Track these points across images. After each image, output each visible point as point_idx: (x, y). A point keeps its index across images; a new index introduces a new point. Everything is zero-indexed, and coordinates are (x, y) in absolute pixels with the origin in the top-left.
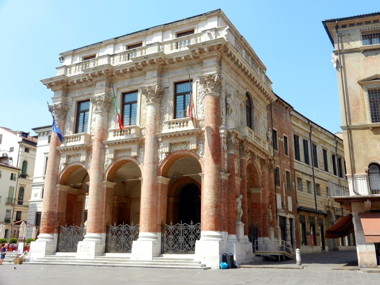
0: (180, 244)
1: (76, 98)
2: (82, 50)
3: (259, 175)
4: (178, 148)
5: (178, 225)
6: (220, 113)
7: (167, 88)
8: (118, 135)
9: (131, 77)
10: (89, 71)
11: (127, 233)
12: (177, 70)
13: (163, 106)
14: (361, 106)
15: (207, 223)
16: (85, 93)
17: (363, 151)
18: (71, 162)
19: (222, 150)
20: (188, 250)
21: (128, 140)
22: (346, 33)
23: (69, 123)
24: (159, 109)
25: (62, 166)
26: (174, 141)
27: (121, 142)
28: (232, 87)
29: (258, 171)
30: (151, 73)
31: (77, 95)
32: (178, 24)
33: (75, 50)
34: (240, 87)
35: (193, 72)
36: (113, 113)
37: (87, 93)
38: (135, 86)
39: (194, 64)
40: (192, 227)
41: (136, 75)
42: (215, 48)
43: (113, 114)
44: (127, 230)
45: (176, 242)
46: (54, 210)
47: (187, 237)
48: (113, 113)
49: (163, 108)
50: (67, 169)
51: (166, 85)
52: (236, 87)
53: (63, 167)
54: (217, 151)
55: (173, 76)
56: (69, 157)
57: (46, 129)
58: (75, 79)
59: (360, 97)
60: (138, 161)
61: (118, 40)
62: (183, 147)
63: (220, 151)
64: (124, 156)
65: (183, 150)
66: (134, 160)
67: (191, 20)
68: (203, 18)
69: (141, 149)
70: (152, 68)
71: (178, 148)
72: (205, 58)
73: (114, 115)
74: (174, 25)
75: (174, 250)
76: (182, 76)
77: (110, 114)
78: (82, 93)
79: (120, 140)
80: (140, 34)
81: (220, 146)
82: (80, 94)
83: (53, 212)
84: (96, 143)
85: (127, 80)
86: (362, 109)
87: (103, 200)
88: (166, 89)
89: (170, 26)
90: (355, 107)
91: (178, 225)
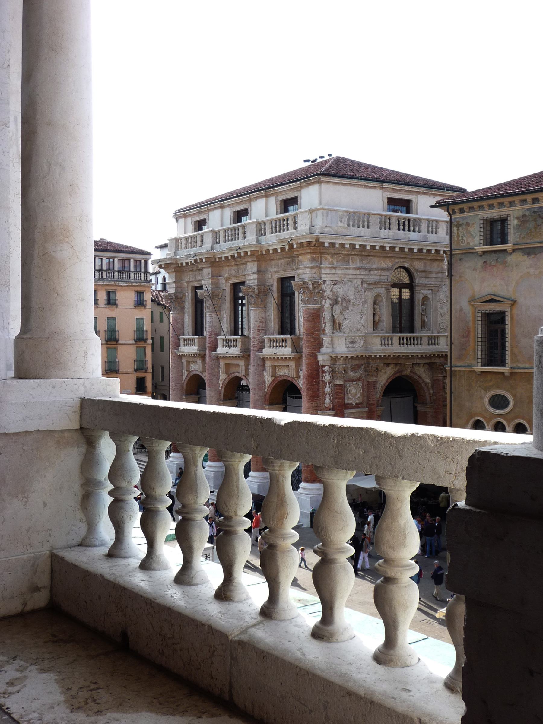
3: (425, 388)
6: (319, 331)
13: (268, 311)
19: (321, 382)
24: (263, 315)
28: (351, 281)
29: (421, 381)
31: (191, 280)
34: (372, 272)
50: (189, 377)
52: (362, 277)
54: (314, 385)
55: (275, 269)
63: (318, 383)
76: (284, 270)
78: (196, 278)
81: (318, 378)
90: (464, 340)
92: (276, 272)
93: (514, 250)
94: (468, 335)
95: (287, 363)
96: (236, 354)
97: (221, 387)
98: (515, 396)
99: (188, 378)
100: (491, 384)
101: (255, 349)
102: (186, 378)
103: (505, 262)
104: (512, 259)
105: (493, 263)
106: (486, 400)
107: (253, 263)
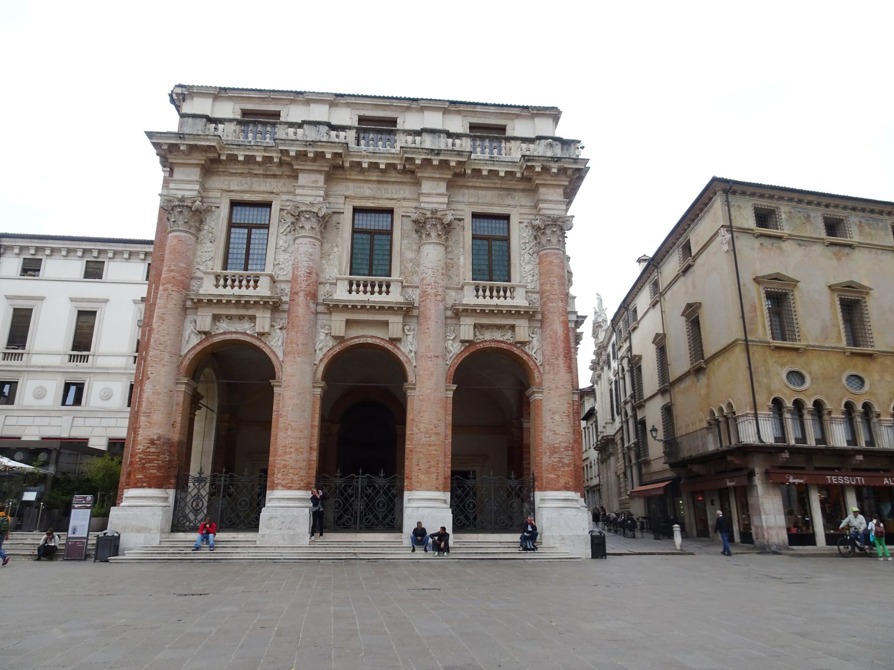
0: (356, 513)
4: (488, 336)
5: (352, 478)
7: (460, 220)
8: (358, 292)
9: (379, 182)
10: (291, 145)
11: (370, 491)
12: (481, 193)
14: (759, 313)
15: (558, 476)
16: (258, 189)
17: (765, 380)
18: (222, 331)
20: (373, 524)
21: (386, 306)
22: (736, 204)
23: (209, 244)
25: (192, 336)
26: (485, 321)
27: (368, 305)
30: (434, 184)
32: (479, 109)
33: (225, 89)
35: (512, 203)
36: (334, 244)
37: (263, 188)
38: (387, 201)
39: (515, 190)
40: (380, 481)
41: (393, 180)
42: (570, 172)
44: (370, 487)
45: (347, 509)
46: (171, 435)
47: (461, 502)
48: (334, 244)
49: (450, 256)
50: (206, 344)
51: (459, 214)
53: (195, 340)
55: (472, 200)
56: (216, 318)
57: (127, 245)
58: (242, 153)
59: (757, 301)
60: (399, 349)
61: (342, 101)
62: (498, 335)
64: (364, 336)
65: (499, 341)
66: (390, 347)
68: (525, 113)
69: (407, 327)
70: (437, 176)
71: (488, 336)
72: (545, 185)
73: (336, 249)
75: (249, 524)
76: (491, 205)
77: (326, 246)
79: (368, 301)
82: (245, 187)
83: (169, 439)
84: (302, 298)
85: (369, 185)
86: (759, 319)
87: (313, 420)
88: (456, 222)
91: (352, 478)
92: (470, 204)
93: (788, 239)
94: (755, 311)
95: (510, 322)
96: (397, 303)
97: (321, 361)
98: (810, 373)
99: (200, 348)
100: (785, 360)
101: (439, 298)
102: (194, 347)
103: (780, 248)
104: (787, 246)
105: (770, 246)
106: (784, 376)
107: (435, 183)
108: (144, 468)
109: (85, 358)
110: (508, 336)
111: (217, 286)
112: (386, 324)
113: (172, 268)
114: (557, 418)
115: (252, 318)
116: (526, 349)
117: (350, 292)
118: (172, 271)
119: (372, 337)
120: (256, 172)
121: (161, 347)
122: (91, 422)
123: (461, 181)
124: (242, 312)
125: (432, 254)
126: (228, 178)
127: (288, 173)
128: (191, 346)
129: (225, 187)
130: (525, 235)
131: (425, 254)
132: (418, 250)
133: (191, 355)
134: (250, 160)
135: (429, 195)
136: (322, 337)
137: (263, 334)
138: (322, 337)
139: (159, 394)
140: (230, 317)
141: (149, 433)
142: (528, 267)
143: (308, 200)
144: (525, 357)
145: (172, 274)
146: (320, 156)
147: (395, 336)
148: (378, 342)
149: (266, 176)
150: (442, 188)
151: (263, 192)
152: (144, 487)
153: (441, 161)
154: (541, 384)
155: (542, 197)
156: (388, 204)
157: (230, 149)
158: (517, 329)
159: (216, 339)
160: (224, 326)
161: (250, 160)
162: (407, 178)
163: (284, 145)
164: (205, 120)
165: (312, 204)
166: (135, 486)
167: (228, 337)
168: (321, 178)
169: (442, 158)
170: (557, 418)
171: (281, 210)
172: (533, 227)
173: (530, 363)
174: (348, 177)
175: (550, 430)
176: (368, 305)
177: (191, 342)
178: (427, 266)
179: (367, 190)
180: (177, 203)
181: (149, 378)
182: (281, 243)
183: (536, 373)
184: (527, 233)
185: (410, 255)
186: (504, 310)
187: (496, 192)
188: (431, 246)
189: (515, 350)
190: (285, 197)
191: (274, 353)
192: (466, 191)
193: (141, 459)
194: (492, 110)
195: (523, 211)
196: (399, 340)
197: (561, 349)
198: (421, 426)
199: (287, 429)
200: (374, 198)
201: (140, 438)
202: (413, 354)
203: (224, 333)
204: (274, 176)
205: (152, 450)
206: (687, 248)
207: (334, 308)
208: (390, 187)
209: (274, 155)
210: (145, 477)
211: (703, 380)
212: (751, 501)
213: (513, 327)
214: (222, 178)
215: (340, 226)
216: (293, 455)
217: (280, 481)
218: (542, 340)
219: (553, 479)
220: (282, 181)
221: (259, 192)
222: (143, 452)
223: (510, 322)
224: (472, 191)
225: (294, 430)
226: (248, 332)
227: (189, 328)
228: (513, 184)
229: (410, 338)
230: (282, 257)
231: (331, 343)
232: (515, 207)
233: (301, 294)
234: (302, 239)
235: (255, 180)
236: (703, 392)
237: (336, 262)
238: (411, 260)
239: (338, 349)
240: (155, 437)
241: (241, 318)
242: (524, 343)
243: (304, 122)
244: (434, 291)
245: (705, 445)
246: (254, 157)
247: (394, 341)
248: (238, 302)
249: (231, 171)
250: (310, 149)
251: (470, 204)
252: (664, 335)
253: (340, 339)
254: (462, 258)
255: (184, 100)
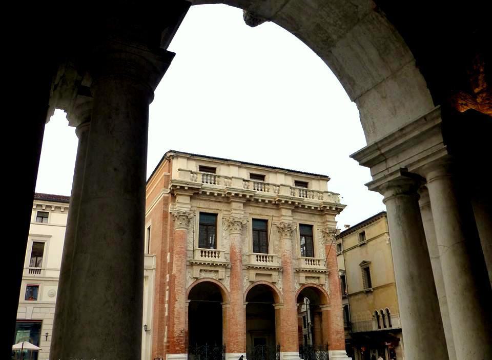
1: (200, 209)
2: (202, 159)
10: (233, 191)
16: (212, 207)
18: (202, 277)
25: (190, 279)
27: (266, 267)
32: (299, 175)
35: (314, 220)
37: (214, 208)
43: (245, 238)
50: (196, 284)
61: (244, 166)
65: (313, 284)
66: (272, 286)
67: (309, 176)
73: (246, 239)
74: (296, 174)
80: (266, 169)
82: (206, 206)
84: (238, 263)
89: (292, 173)
92: (299, 220)
95: (318, 275)
102: (191, 285)
108: (179, 344)
109: (39, 271)
110: (316, 282)
111: (202, 256)
112: (270, 275)
113: (182, 246)
114: (339, 318)
115: (217, 271)
116: (324, 288)
117: (257, 260)
118: (182, 248)
119: (265, 281)
120: (211, 199)
121: (181, 285)
122: (43, 310)
123: (296, 210)
124: (213, 269)
125: (287, 244)
126: (199, 201)
127: (226, 201)
128: (190, 285)
129: (198, 206)
130: (320, 235)
131: (284, 243)
132: (280, 241)
133: (190, 289)
134: (212, 194)
135: (286, 216)
136: (245, 281)
137: (220, 279)
138: (245, 281)
139: (182, 308)
140: (206, 271)
141: (180, 327)
142: (322, 250)
143: (238, 216)
144: (323, 291)
145: (183, 249)
146: (244, 196)
147: (274, 281)
148: (267, 283)
149: (216, 201)
150: (289, 213)
151: (214, 209)
152: (180, 353)
153: (292, 202)
154: (330, 303)
155: (328, 219)
156: (266, 218)
157: (204, 189)
158: (321, 279)
159: (200, 281)
160: (204, 275)
161: (212, 194)
162: (274, 207)
163: (230, 190)
164: (190, 173)
165: (240, 218)
166: (175, 352)
167: (205, 280)
168: (242, 205)
169: (292, 201)
170: (339, 318)
171: (223, 218)
172: (323, 232)
173: (325, 294)
174: (251, 204)
175: (336, 324)
176: (266, 267)
177: (190, 283)
178: (285, 247)
179: (258, 211)
180: (182, 214)
181: (177, 301)
182: (224, 234)
183: (327, 298)
184: (321, 234)
185: (277, 243)
186: (317, 271)
187: (308, 215)
188: (287, 240)
189: (319, 288)
190: (225, 212)
191: (226, 288)
192: (297, 214)
193: (177, 340)
194: (304, 175)
195: (319, 224)
196: (275, 283)
197: (338, 288)
198: (289, 323)
199: (237, 325)
200: (261, 215)
201: (175, 330)
202: (281, 289)
203: (204, 278)
204: (219, 202)
205: (182, 335)
206: (363, 234)
207: (250, 268)
208: (267, 210)
209: (222, 193)
210: (180, 348)
211: (371, 297)
212: (397, 351)
213: (318, 278)
214: (196, 201)
215: (248, 227)
216: (241, 337)
217: (236, 349)
218: (329, 284)
219: (337, 345)
220: (223, 204)
221: (212, 209)
222: (178, 336)
223: (318, 275)
224: (300, 214)
225: (240, 325)
226: (214, 278)
227: (189, 275)
228: (315, 212)
229: (280, 282)
230: (225, 241)
231: (249, 284)
232: (315, 222)
233: (238, 261)
234: (236, 235)
235: (211, 203)
236: (371, 302)
237: (247, 245)
238: (277, 245)
239: (251, 287)
240: (182, 329)
241: (211, 271)
242: (322, 285)
243: (233, 177)
244: (290, 261)
245: (371, 325)
246: (214, 193)
247: (274, 283)
248: (213, 264)
249: (201, 198)
250: (241, 193)
251: (299, 220)
252: (345, 272)
253: (252, 282)
254: (297, 245)
255: (173, 158)
